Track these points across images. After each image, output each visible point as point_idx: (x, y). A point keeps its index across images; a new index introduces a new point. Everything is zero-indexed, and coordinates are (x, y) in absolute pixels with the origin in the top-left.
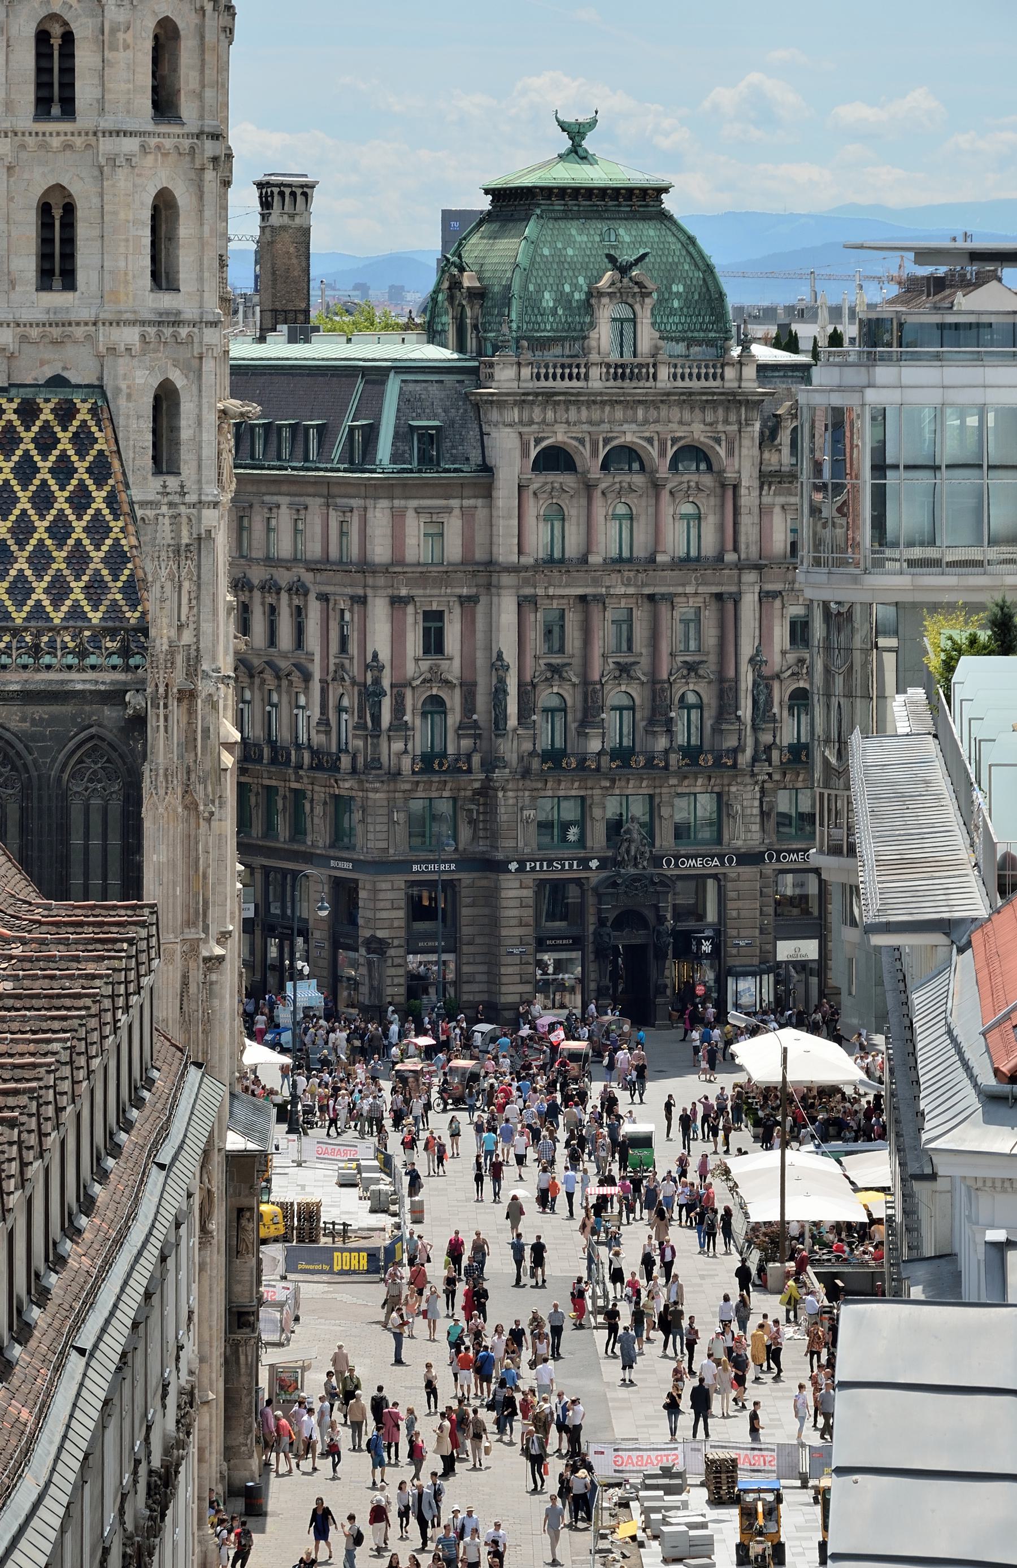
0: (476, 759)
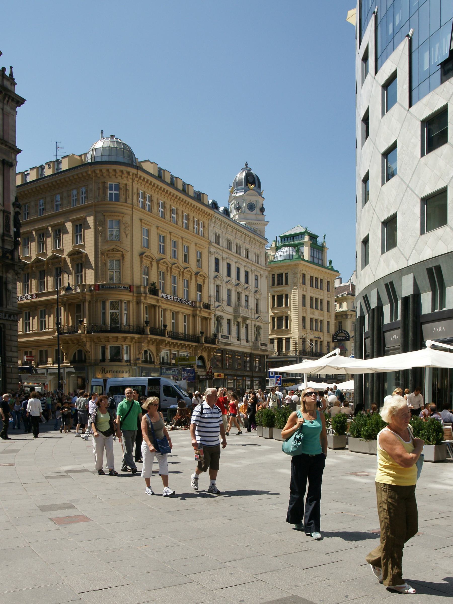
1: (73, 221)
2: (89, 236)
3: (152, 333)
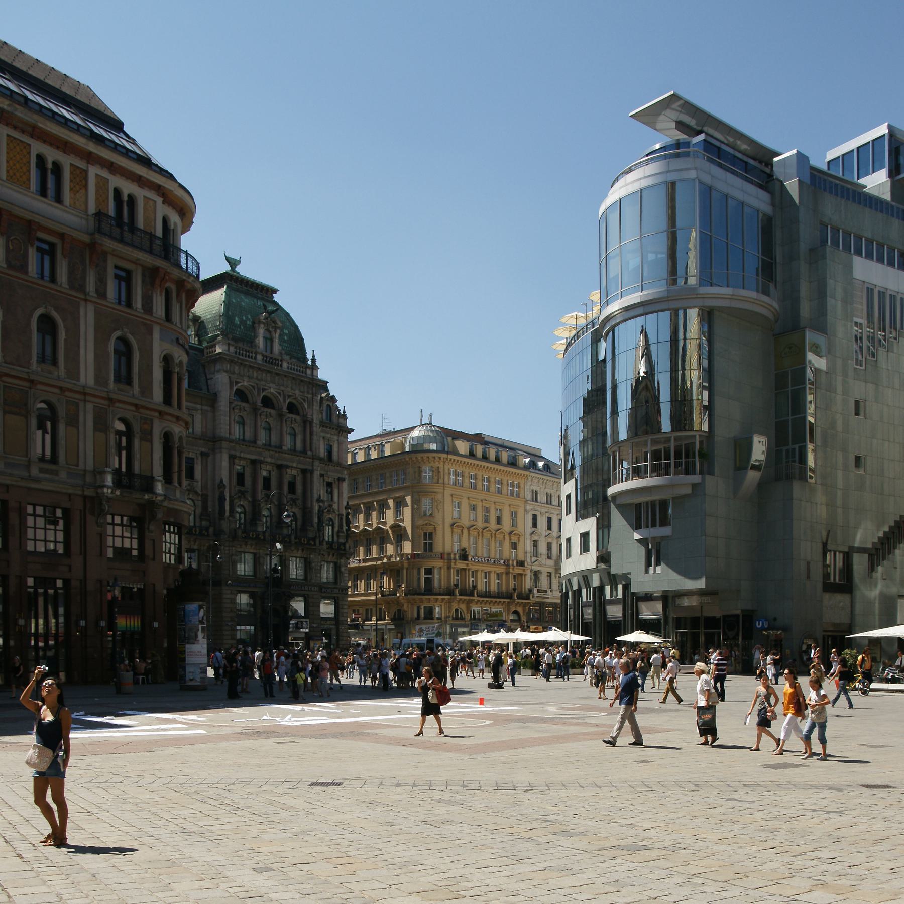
0: (211, 530)
1: (394, 499)
2: (407, 512)
3: (460, 595)
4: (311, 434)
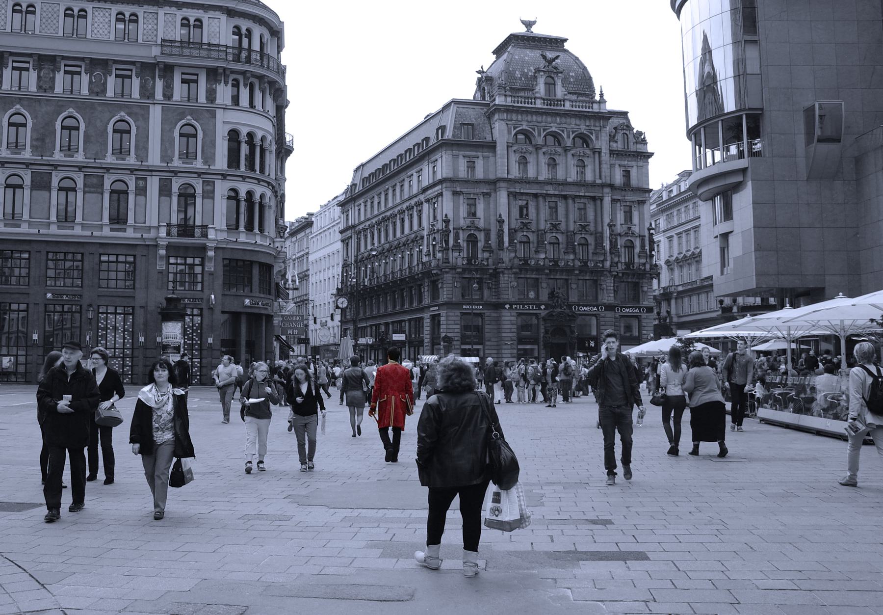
4: (600, 164)
